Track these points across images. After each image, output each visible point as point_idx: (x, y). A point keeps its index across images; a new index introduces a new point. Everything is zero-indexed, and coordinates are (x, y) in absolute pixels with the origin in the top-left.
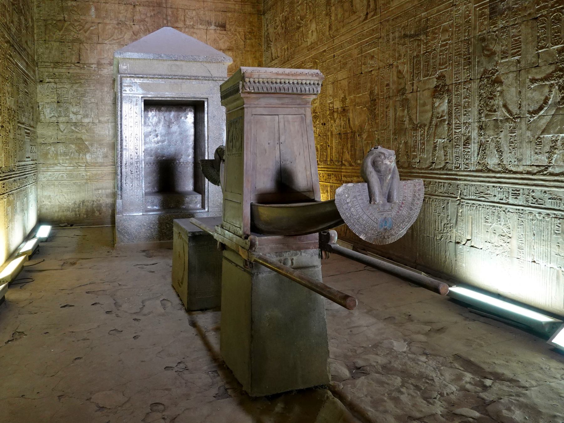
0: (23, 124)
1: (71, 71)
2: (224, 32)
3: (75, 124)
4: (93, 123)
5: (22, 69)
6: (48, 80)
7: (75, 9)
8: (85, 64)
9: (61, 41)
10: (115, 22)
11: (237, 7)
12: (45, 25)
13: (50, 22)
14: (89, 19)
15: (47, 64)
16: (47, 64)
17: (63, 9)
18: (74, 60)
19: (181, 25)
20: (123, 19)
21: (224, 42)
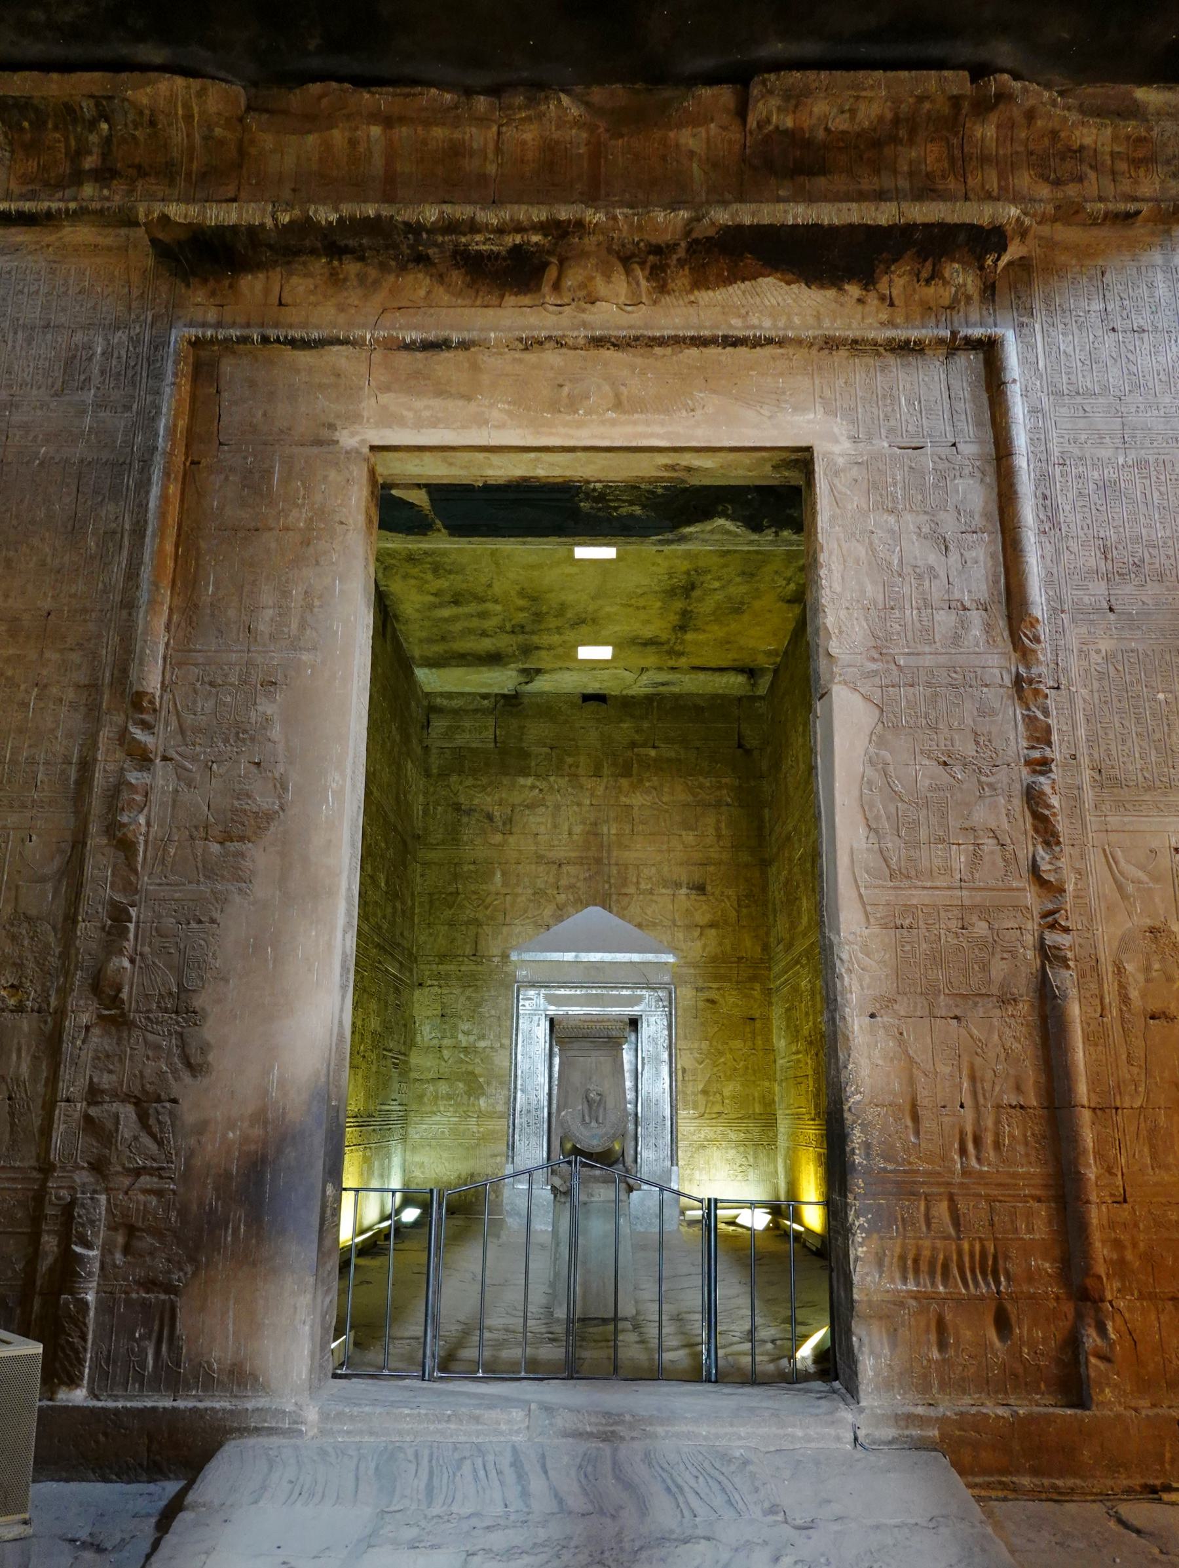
0: (390, 1051)
1: (463, 968)
2: (703, 898)
3: (466, 1050)
4: (492, 1048)
5: (393, 975)
6: (429, 982)
7: (473, 875)
8: (483, 956)
9: (452, 924)
10: (530, 891)
11: (725, 856)
12: (431, 902)
13: (436, 896)
14: (492, 889)
15: (431, 958)
16: (431, 958)
17: (456, 877)
18: (468, 950)
19: (631, 890)
20: (542, 886)
21: (703, 914)
